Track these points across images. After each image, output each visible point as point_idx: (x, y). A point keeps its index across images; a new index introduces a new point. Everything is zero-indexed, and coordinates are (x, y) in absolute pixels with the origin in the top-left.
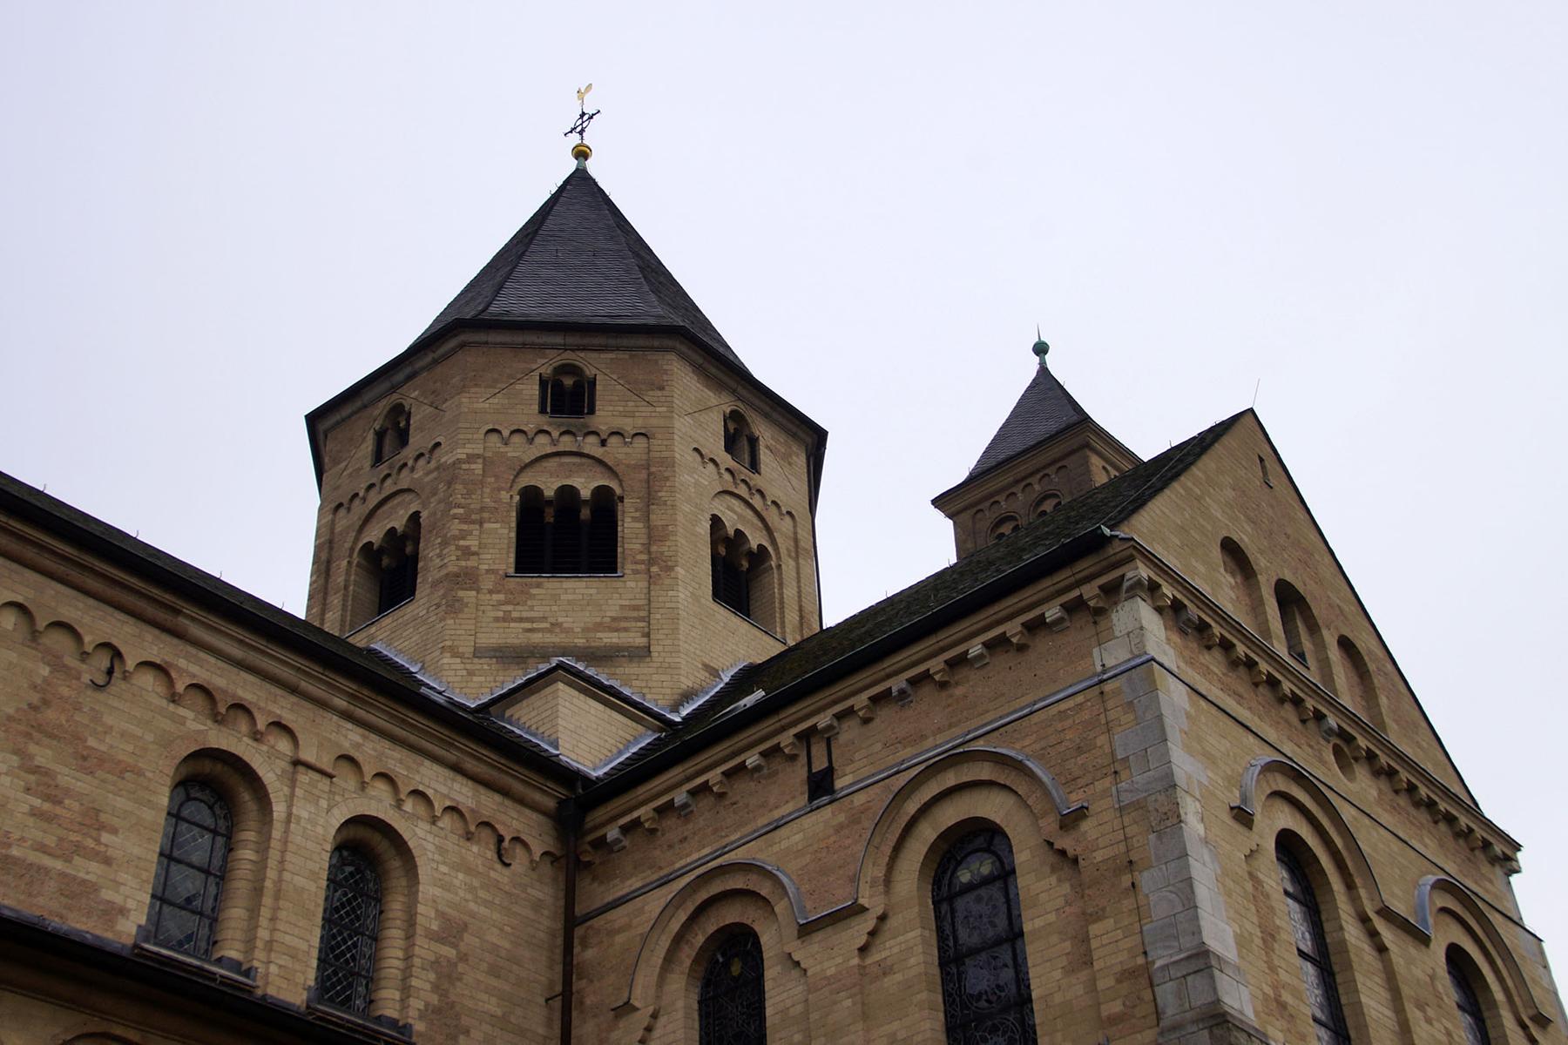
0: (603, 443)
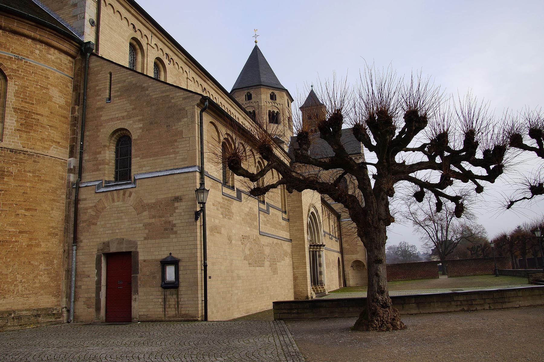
0: (278, 105)
